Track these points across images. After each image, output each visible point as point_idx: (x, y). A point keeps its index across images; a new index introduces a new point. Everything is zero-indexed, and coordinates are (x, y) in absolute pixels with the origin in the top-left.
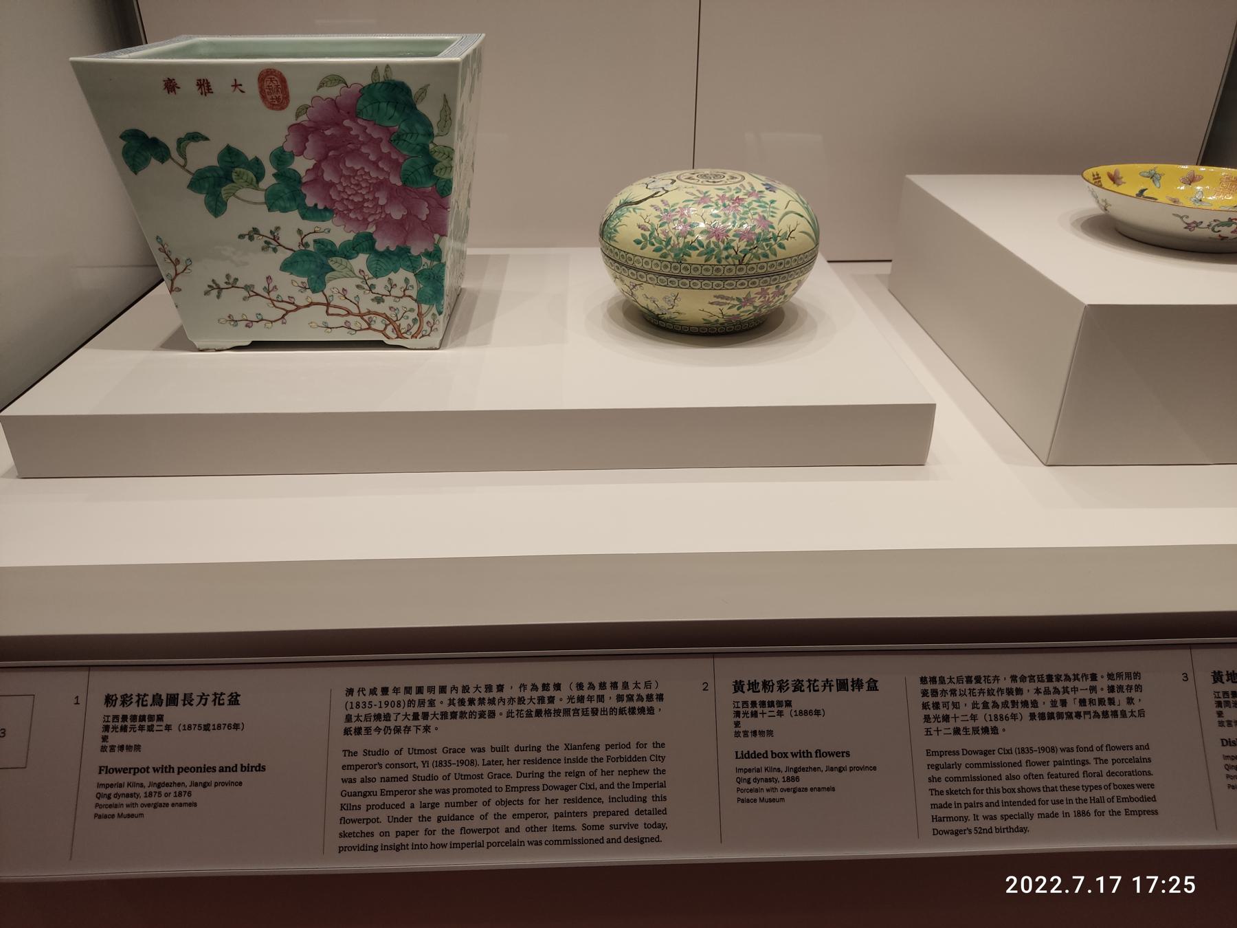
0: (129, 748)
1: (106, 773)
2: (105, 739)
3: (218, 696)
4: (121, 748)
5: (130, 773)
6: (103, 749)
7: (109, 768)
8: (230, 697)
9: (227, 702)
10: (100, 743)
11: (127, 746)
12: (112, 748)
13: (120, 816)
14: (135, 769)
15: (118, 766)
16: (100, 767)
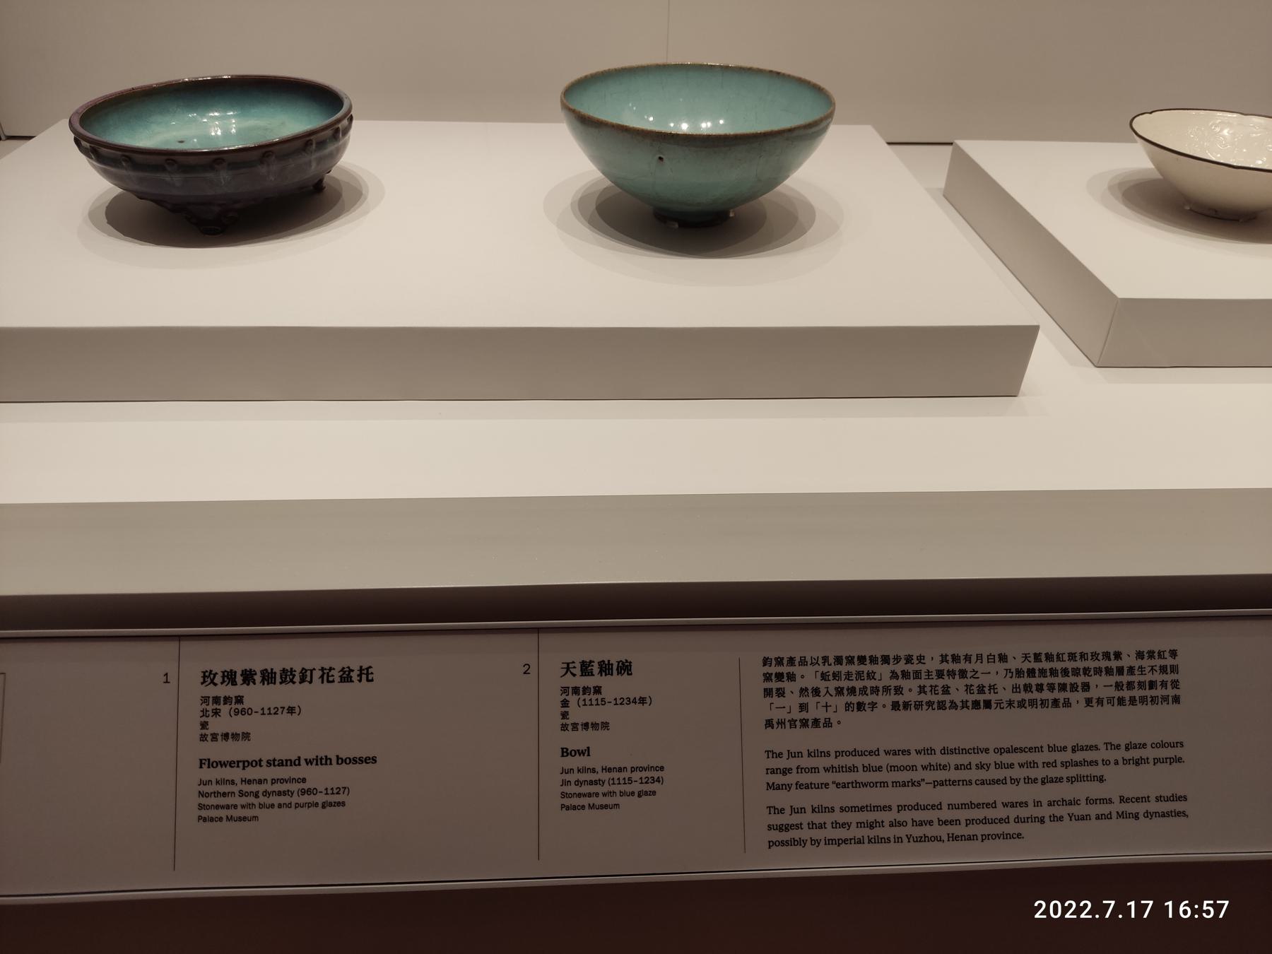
0: (235, 736)
1: (209, 767)
2: (204, 725)
3: (325, 671)
4: (226, 736)
5: (238, 766)
6: (203, 738)
7: (211, 761)
8: (342, 673)
9: (337, 679)
10: (198, 731)
11: (233, 734)
12: (214, 737)
13: (229, 819)
14: (244, 762)
15: (224, 759)
16: (201, 760)
